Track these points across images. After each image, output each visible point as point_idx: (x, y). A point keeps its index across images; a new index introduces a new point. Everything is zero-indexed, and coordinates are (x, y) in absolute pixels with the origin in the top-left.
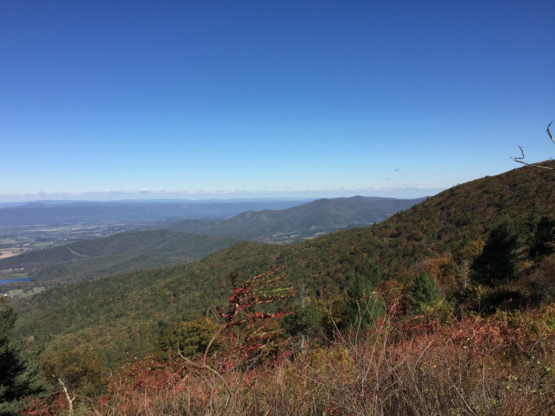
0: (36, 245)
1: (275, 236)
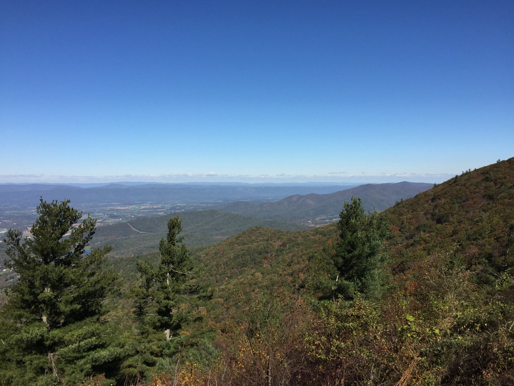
0: (107, 221)
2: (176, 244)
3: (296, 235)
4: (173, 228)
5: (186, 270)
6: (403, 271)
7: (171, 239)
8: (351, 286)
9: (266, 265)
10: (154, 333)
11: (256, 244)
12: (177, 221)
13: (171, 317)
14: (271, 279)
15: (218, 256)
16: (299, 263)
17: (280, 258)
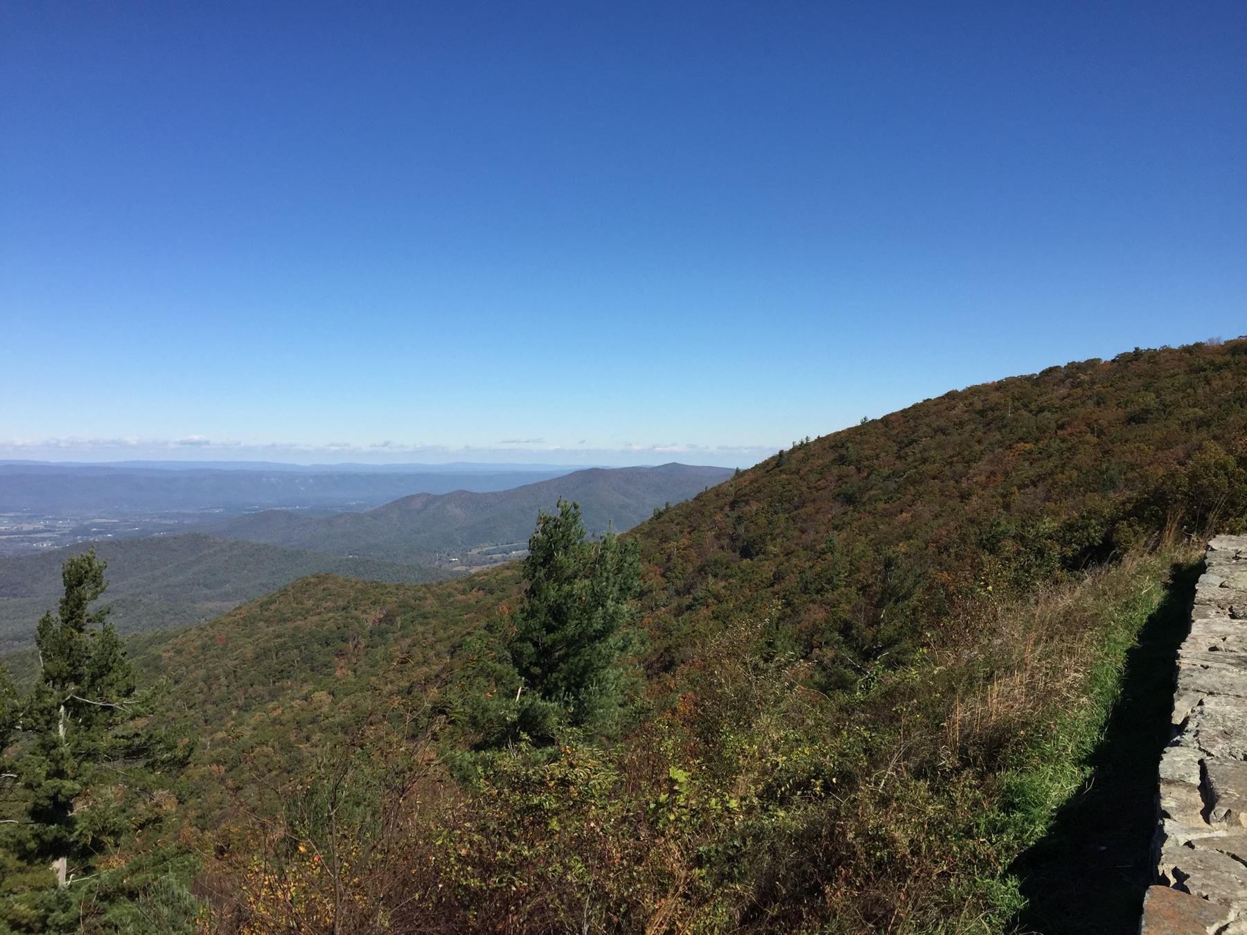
1: (475, 552)
2: (88, 627)
3: (420, 594)
4: (80, 583)
5: (115, 697)
6: (669, 666)
7: (72, 613)
8: (553, 711)
9: (342, 672)
10: (20, 870)
11: (316, 618)
12: (90, 564)
13: (71, 823)
14: (354, 707)
15: (209, 654)
16: (426, 662)
17: (380, 650)
